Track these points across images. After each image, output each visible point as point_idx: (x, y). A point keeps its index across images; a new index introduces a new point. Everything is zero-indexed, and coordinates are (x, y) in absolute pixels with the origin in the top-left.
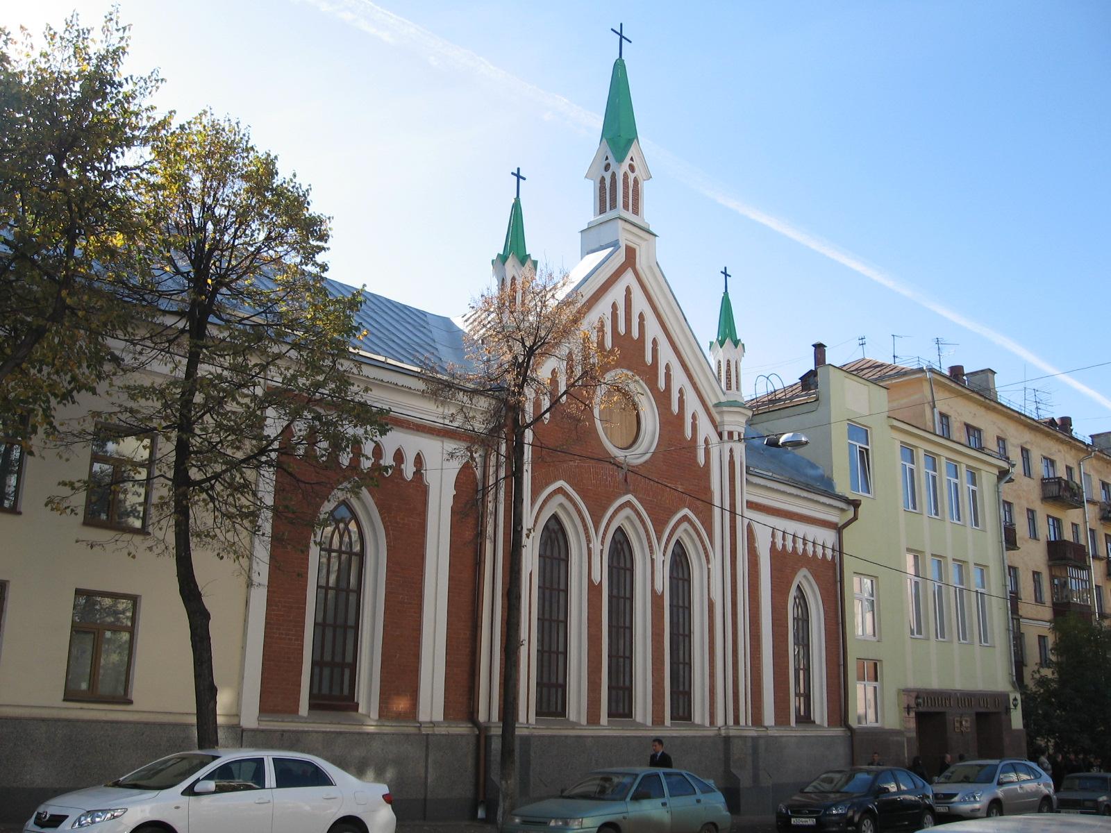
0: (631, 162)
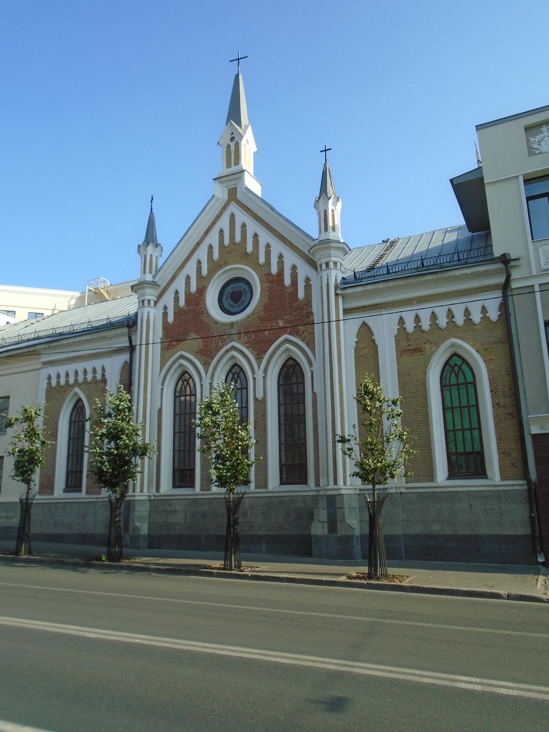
0: (232, 136)
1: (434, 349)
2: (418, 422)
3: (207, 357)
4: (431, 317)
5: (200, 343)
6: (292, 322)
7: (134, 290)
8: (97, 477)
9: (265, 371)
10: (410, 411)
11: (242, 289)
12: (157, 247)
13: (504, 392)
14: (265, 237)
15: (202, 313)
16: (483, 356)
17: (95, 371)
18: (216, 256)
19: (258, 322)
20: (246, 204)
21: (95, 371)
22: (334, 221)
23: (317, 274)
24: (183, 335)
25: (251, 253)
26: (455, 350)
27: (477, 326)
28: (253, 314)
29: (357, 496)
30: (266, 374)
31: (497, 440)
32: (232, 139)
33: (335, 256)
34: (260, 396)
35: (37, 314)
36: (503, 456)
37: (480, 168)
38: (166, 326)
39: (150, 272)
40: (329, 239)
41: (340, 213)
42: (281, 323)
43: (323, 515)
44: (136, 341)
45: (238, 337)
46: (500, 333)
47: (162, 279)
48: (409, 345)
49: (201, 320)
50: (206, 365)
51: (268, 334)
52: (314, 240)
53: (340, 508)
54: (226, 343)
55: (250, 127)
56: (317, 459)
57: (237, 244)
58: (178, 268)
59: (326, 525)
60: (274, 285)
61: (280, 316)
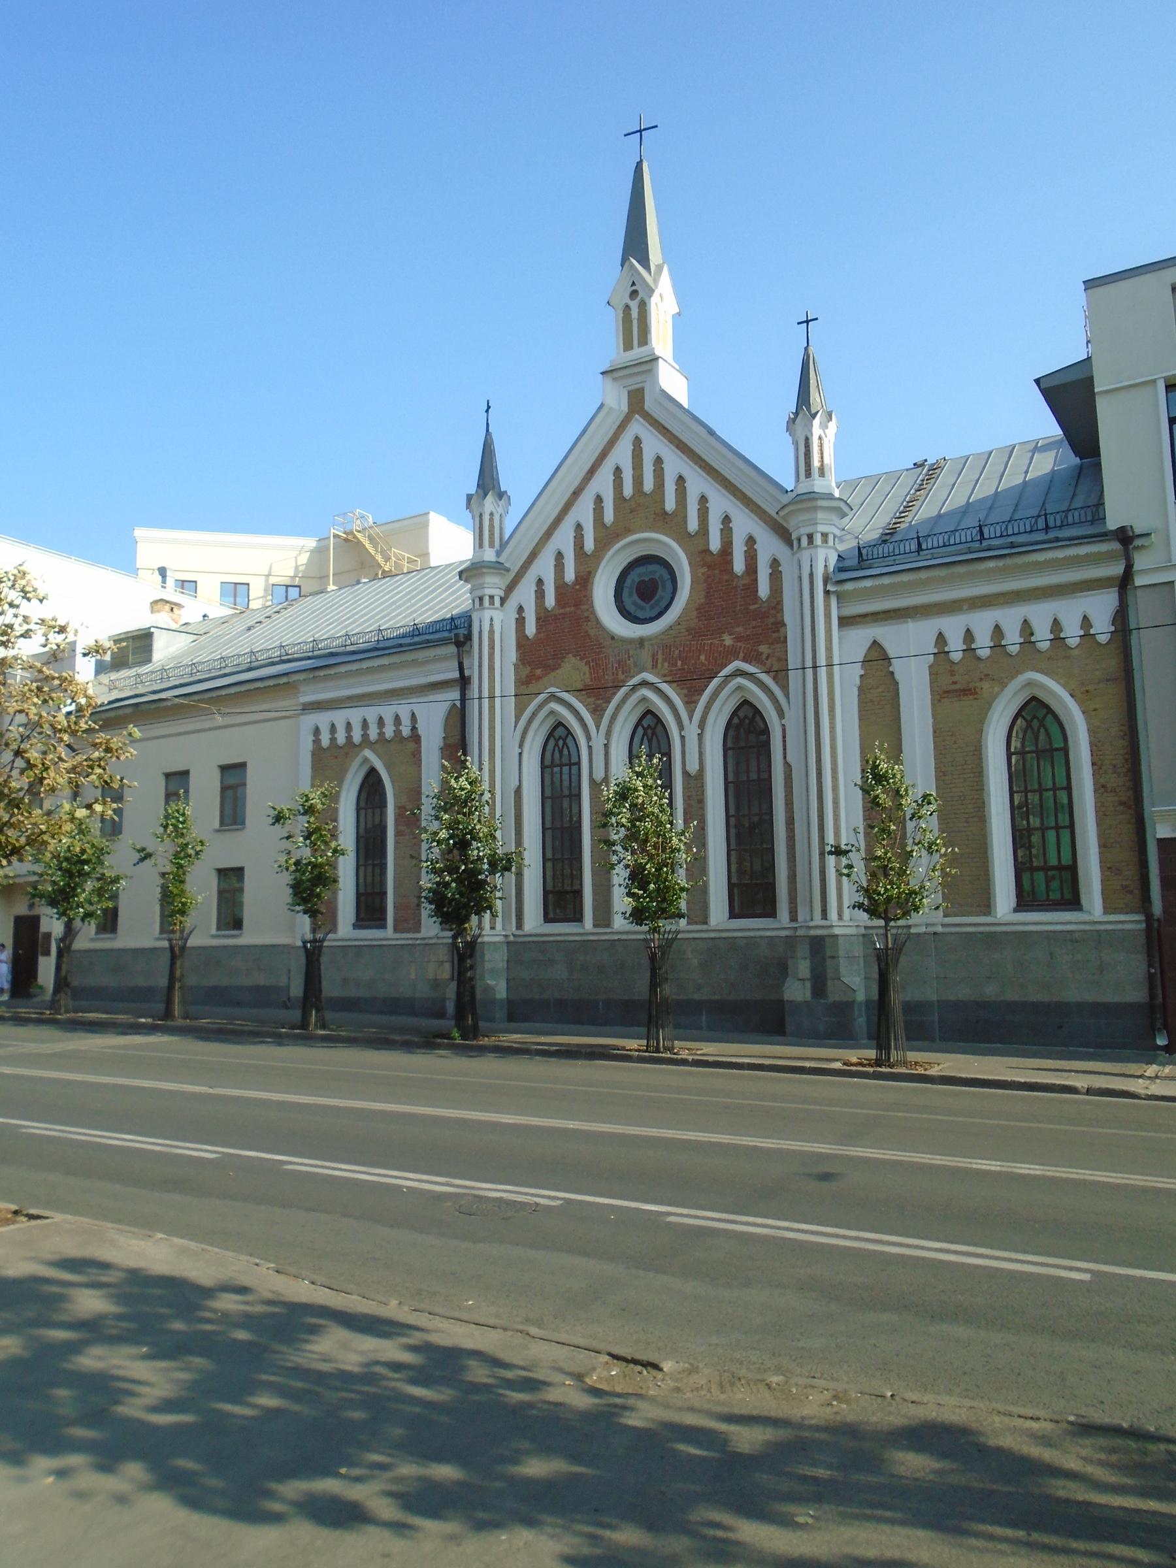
0: (634, 288)
1: (996, 689)
2: (967, 816)
3: (598, 699)
4: (994, 632)
5: (584, 674)
6: (749, 640)
7: (464, 576)
8: (433, 907)
9: (702, 725)
10: (952, 797)
11: (657, 577)
12: (500, 500)
13: (1114, 766)
14: (697, 484)
15: (587, 619)
16: (1080, 703)
17: (397, 720)
18: (609, 516)
19: (688, 638)
20: (660, 420)
21: (397, 720)
22: (822, 458)
23: (793, 554)
24: (554, 659)
25: (673, 512)
26: (1034, 692)
27: (1072, 651)
28: (679, 624)
29: (861, 938)
30: (702, 730)
31: (1100, 847)
32: (634, 294)
33: (825, 524)
34: (693, 768)
35: (238, 586)
36: (1108, 873)
37: (1089, 358)
38: (523, 643)
39: (492, 545)
40: (814, 492)
41: (833, 440)
42: (728, 641)
43: (803, 968)
44: (472, 672)
45: (653, 665)
46: (1112, 664)
47: (514, 559)
48: (954, 683)
49: (586, 632)
50: (597, 712)
51: (706, 660)
52: (787, 491)
53: (833, 957)
54: (632, 674)
55: (665, 268)
56: (792, 877)
57: (646, 494)
58: (541, 538)
59: (808, 984)
60: (717, 572)
61: (727, 628)
